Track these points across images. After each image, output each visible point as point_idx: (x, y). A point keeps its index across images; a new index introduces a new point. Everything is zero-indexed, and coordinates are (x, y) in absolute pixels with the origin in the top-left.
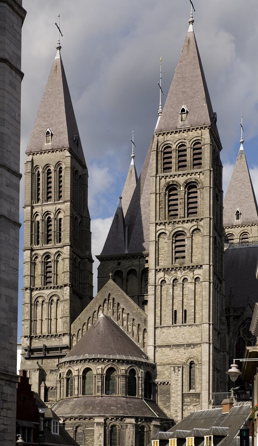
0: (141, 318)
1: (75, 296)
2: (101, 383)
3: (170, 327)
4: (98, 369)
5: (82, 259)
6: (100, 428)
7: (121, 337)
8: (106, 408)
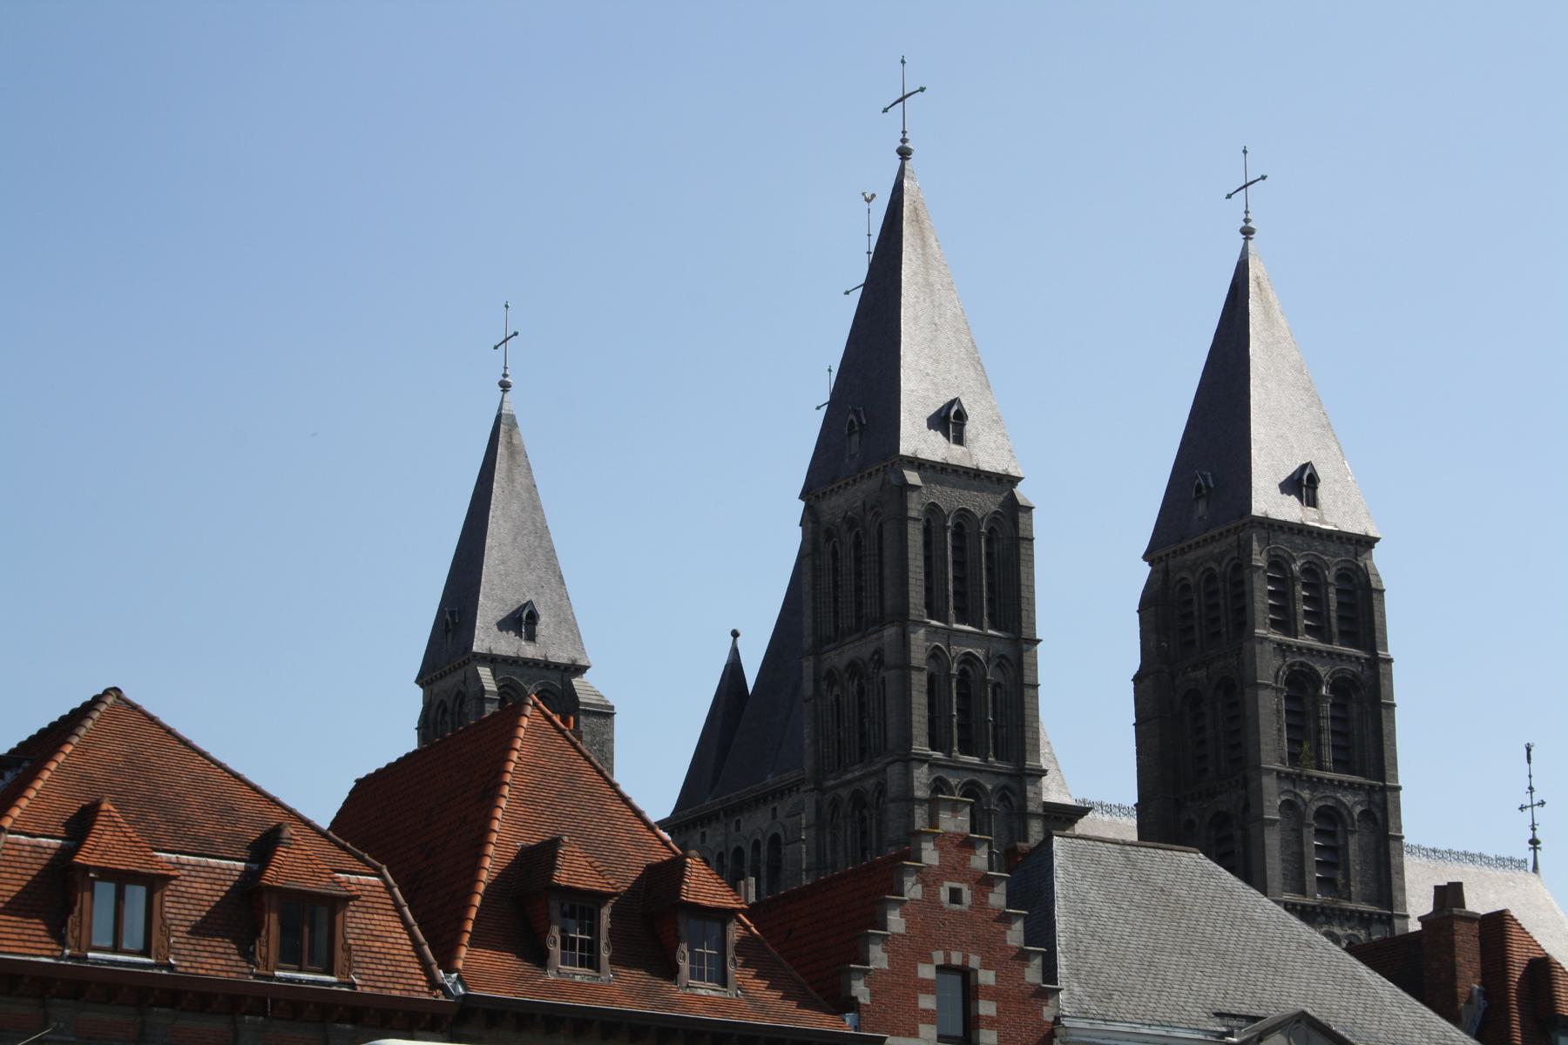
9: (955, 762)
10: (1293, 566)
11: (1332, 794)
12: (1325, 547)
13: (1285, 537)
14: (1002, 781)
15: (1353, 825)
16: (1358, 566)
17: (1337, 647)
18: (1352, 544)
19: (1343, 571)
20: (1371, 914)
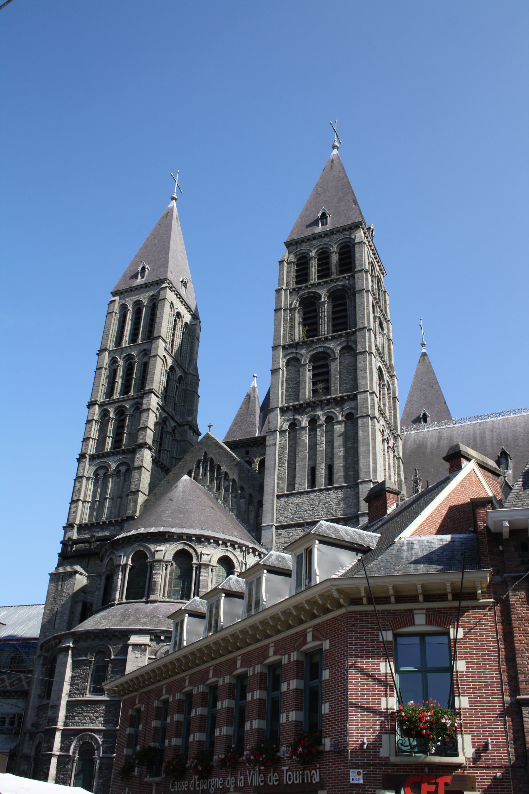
0: (254, 485)
1: (159, 469)
2: (160, 576)
3: (302, 493)
4: (157, 551)
5: (180, 425)
6: (139, 656)
7: (212, 508)
8: (161, 620)
9: (112, 400)
10: (310, 254)
11: (322, 345)
12: (331, 238)
13: (307, 244)
14: (132, 402)
15: (335, 356)
16: (350, 238)
17: (334, 276)
18: (347, 231)
19: (344, 244)
20: (341, 397)
